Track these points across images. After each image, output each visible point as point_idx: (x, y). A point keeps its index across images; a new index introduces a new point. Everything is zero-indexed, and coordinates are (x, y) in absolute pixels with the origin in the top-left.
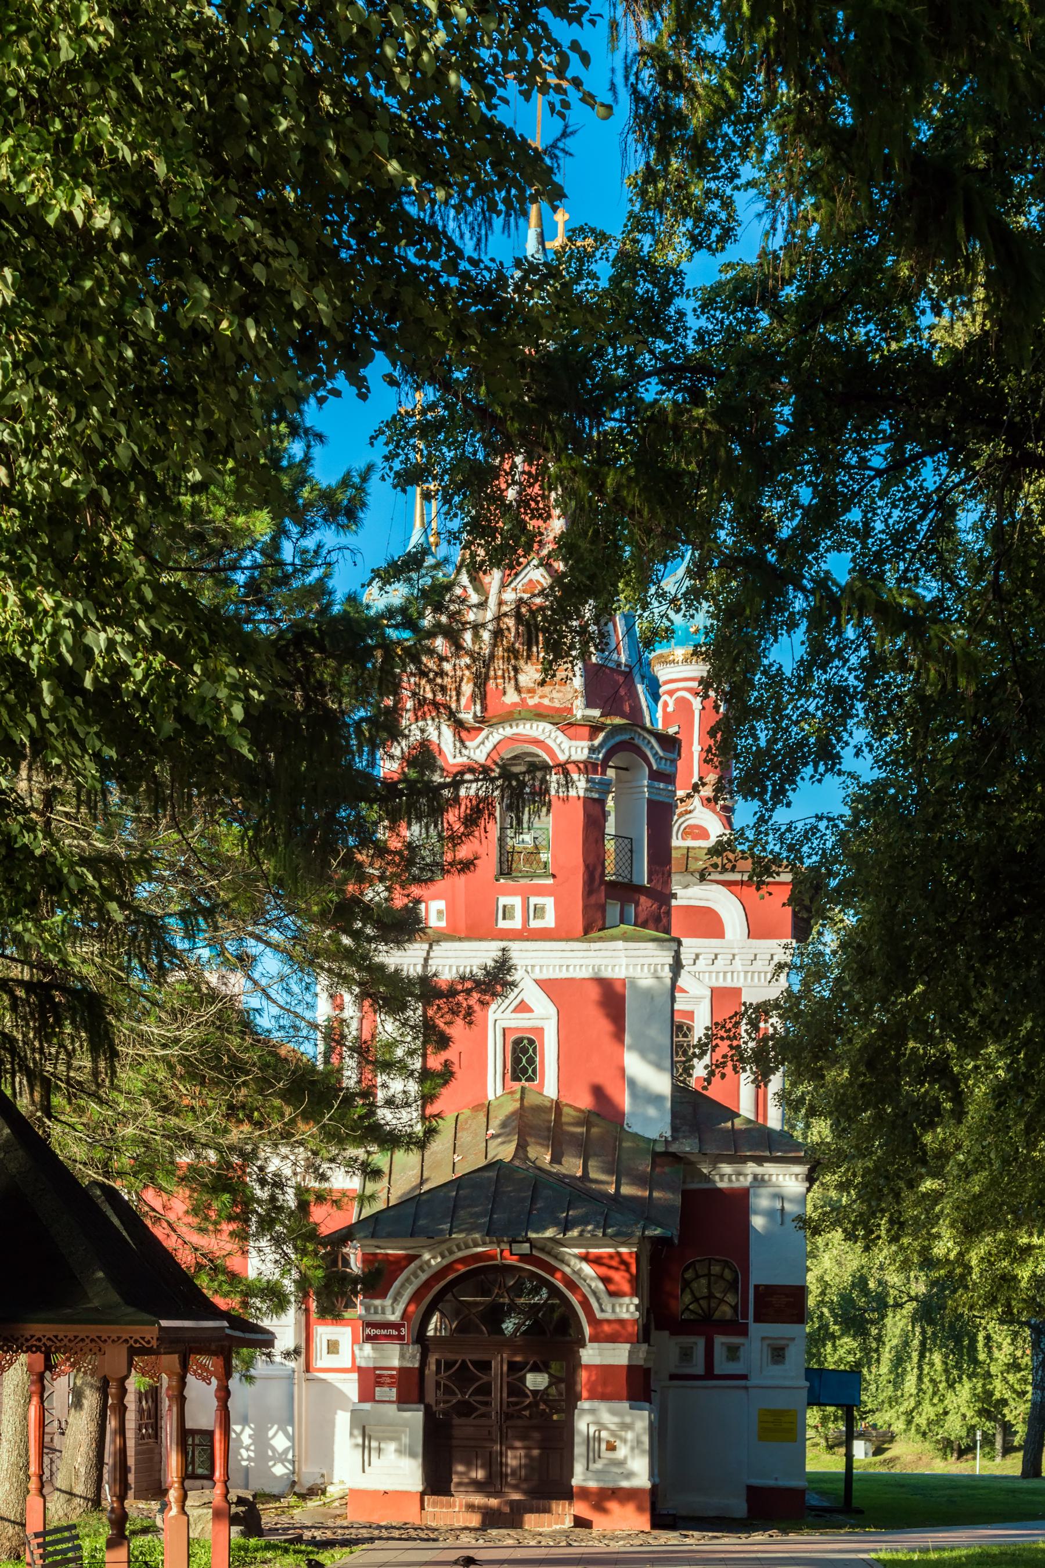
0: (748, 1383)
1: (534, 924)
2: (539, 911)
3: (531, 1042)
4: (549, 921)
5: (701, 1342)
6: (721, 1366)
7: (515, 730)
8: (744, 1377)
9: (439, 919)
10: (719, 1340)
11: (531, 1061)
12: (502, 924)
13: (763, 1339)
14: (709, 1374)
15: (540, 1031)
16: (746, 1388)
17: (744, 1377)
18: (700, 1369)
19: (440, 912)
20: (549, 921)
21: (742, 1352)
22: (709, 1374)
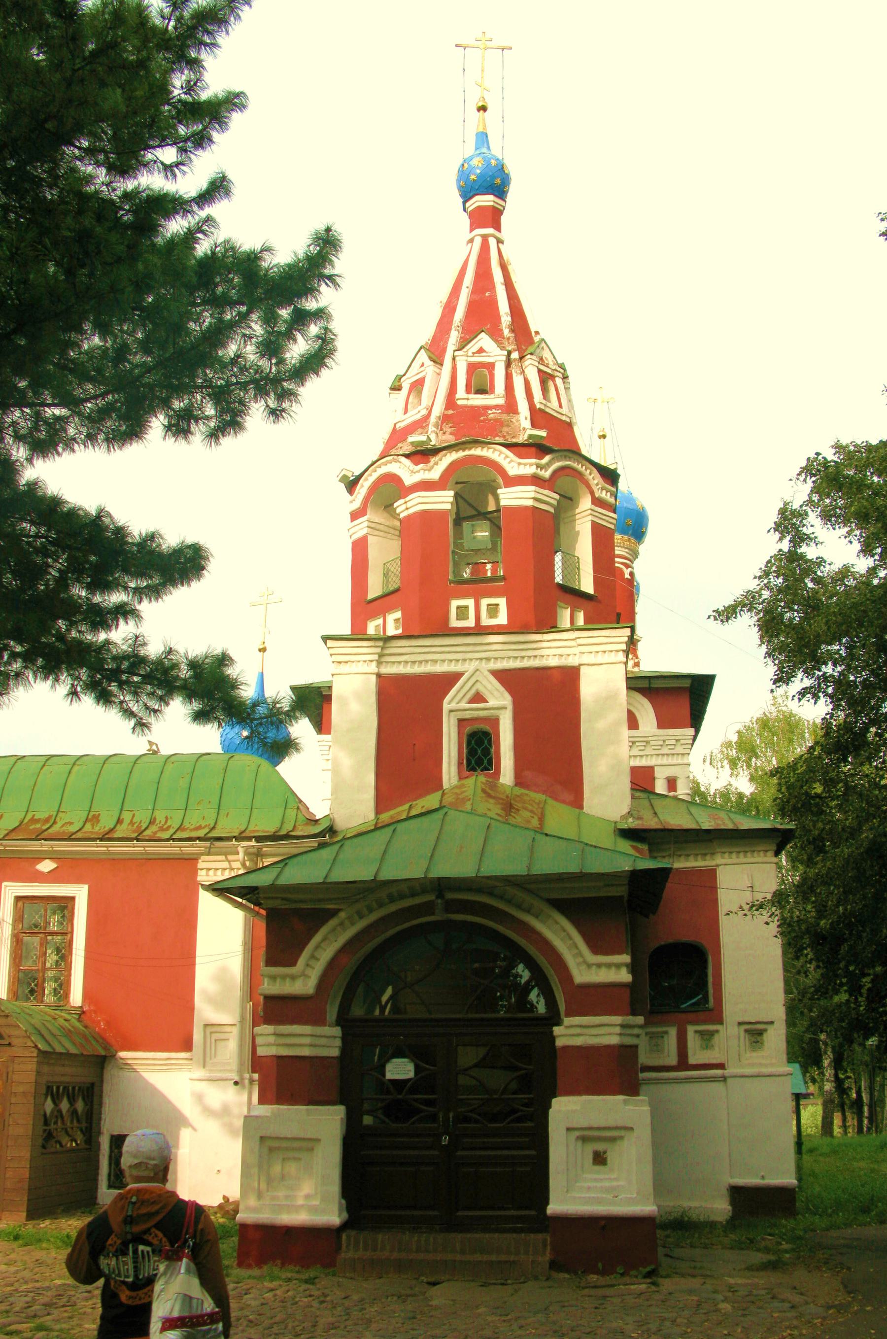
0: (726, 1072)
1: (486, 621)
2: (493, 610)
3: (486, 734)
4: (502, 619)
5: (673, 1032)
7: (467, 453)
8: (721, 1066)
9: (397, 628)
10: (691, 1030)
11: (487, 752)
12: (454, 623)
13: (740, 1024)
14: (683, 1064)
15: (495, 722)
16: (724, 1079)
17: (721, 1066)
18: (673, 1060)
19: (396, 620)
20: (502, 619)
22: (683, 1064)
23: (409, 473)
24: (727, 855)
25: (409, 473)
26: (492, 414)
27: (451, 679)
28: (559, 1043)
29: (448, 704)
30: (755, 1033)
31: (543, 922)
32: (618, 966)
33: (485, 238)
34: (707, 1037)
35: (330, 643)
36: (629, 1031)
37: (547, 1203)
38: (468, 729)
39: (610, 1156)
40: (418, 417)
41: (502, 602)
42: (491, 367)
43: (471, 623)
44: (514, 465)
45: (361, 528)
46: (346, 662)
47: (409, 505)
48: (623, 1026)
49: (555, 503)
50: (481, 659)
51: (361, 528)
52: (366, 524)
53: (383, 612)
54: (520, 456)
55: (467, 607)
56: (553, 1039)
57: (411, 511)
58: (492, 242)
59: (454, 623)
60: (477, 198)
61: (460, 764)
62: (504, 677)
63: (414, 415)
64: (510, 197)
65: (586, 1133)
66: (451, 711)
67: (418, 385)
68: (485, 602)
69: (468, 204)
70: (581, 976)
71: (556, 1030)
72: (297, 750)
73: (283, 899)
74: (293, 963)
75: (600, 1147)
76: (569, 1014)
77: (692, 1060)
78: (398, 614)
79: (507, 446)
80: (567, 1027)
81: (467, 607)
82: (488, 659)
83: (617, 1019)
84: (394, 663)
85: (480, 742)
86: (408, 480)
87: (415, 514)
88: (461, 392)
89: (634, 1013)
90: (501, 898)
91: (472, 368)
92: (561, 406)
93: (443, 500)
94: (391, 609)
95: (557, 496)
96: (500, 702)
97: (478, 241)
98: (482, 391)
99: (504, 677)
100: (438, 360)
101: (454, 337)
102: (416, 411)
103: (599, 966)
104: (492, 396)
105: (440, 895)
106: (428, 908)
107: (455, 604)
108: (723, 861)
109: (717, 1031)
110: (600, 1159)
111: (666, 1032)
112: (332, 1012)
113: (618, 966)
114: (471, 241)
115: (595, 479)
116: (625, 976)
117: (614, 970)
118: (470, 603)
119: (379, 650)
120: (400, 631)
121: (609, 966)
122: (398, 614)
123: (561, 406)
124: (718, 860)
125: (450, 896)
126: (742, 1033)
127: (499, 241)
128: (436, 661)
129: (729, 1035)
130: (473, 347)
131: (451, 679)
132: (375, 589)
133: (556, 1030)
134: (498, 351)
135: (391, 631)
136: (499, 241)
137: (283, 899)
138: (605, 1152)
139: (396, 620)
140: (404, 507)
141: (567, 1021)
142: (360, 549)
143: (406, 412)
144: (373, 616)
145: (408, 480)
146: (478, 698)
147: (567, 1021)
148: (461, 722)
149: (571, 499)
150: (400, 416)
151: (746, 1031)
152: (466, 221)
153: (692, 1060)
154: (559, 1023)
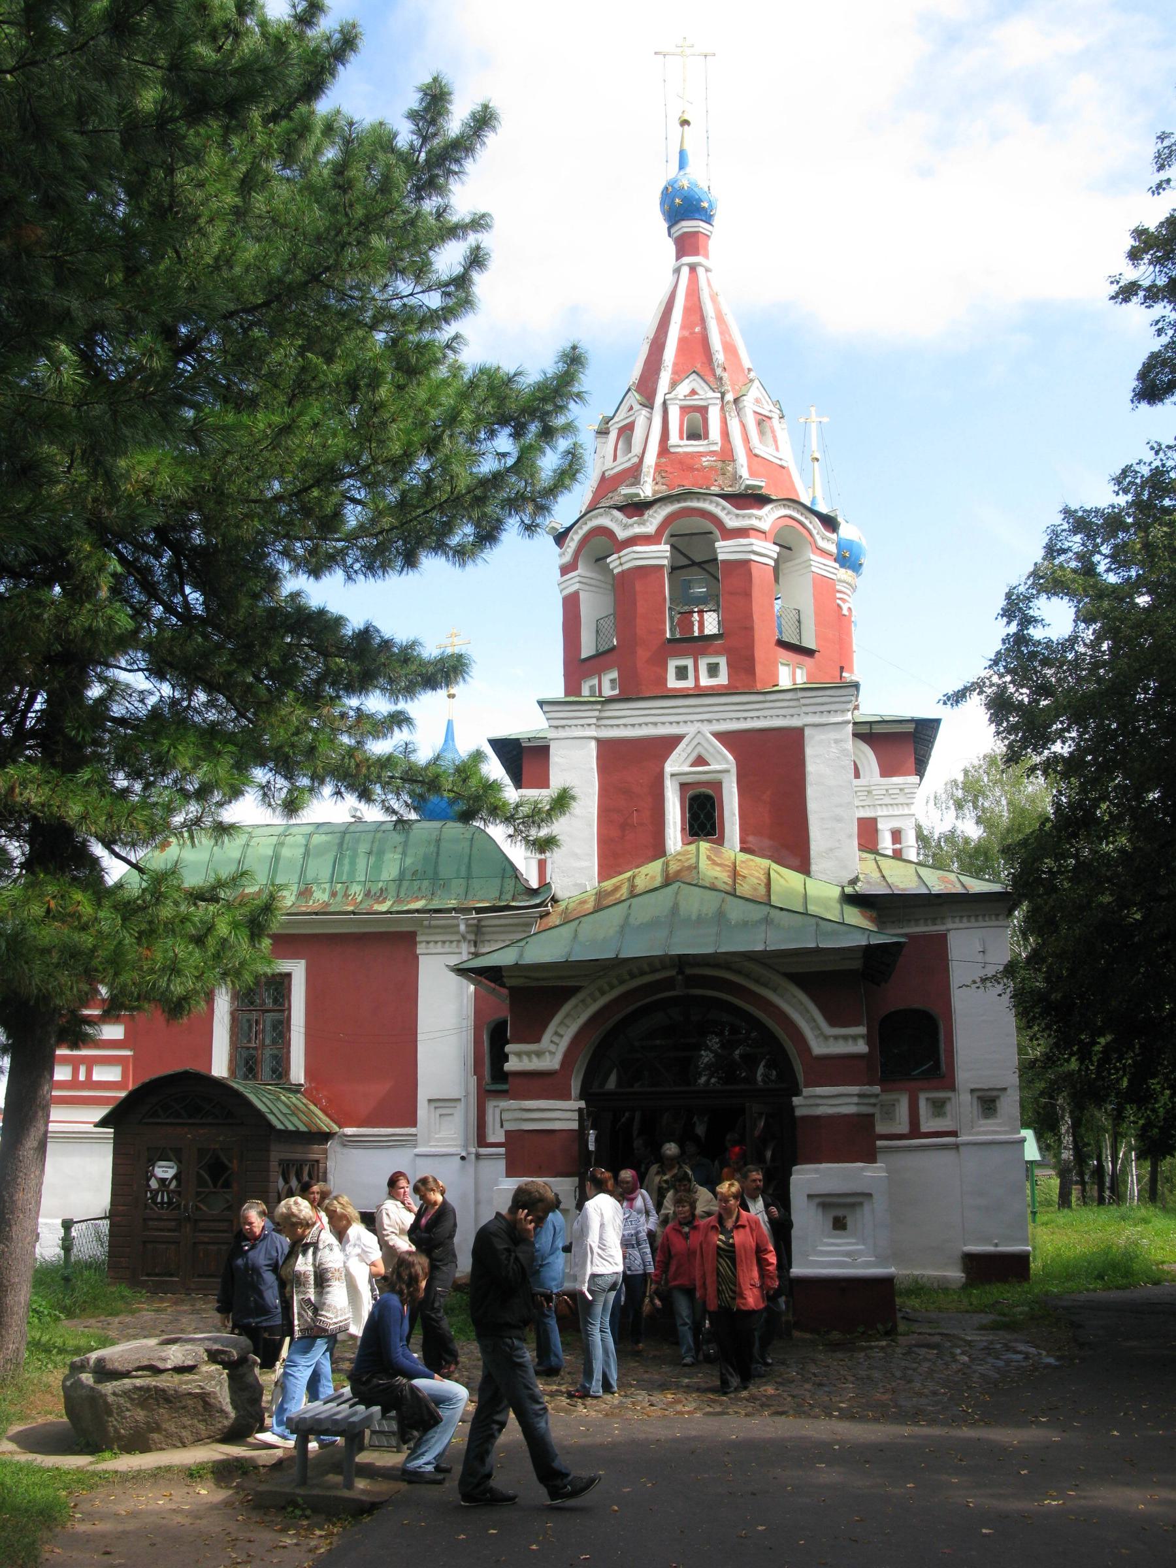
1: (705, 681)
4: (723, 679)
6: (928, 1124)
8: (954, 1134)
9: (613, 689)
12: (673, 683)
13: (972, 1091)
14: (915, 1131)
15: (718, 785)
16: (956, 1147)
17: (954, 1134)
18: (904, 1128)
19: (612, 681)
20: (723, 679)
21: (948, 1107)
22: (915, 1131)
23: (621, 526)
24: (957, 920)
25: (621, 526)
26: (706, 461)
27: (671, 742)
28: (799, 1112)
29: (670, 767)
30: (988, 1103)
31: (782, 996)
32: (855, 1038)
33: (693, 268)
34: (939, 1107)
35: (546, 708)
36: (866, 1101)
37: (790, 1267)
38: (691, 793)
39: (850, 1222)
40: (628, 465)
41: (722, 661)
42: (703, 410)
43: (689, 683)
44: (731, 518)
45: (573, 582)
46: (563, 727)
47: (623, 560)
48: (859, 1096)
49: (775, 556)
50: (702, 721)
51: (573, 582)
52: (578, 579)
53: (599, 672)
54: (738, 508)
55: (686, 668)
56: (792, 1109)
57: (626, 567)
58: (701, 271)
59: (673, 683)
60: (684, 223)
61: (683, 829)
62: (724, 737)
63: (624, 462)
64: (716, 221)
65: (828, 1200)
66: (672, 775)
67: (627, 430)
68: (703, 664)
69: (672, 231)
70: (819, 1048)
71: (796, 1100)
72: (558, 846)
73: (526, 977)
74: (537, 1040)
75: (840, 1213)
76: (806, 1086)
77: (924, 1128)
78: (614, 674)
79: (724, 497)
80: (805, 1098)
81: (686, 668)
82: (709, 721)
83: (855, 1089)
84: (612, 726)
85: (702, 806)
86: (621, 534)
87: (629, 569)
88: (674, 438)
89: (871, 1083)
90: (739, 972)
91: (684, 410)
92: (777, 449)
93: (660, 553)
94: (606, 668)
95: (777, 549)
96: (724, 763)
97: (685, 271)
98: (694, 435)
99: (724, 737)
100: (649, 404)
101: (665, 378)
102: (626, 458)
103: (836, 1038)
104: (706, 442)
105: (681, 972)
106: (669, 983)
107: (672, 664)
108: (955, 926)
109: (949, 1099)
110: (839, 1224)
111: (898, 1100)
112: (575, 1086)
113: (855, 1038)
114: (677, 271)
115: (815, 526)
116: (861, 1047)
117: (851, 1042)
118: (689, 662)
119: (596, 714)
120: (616, 692)
121: (845, 1038)
122: (614, 674)
123: (777, 449)
124: (950, 926)
125: (688, 971)
126: (975, 1101)
127: (707, 270)
128: (655, 724)
129: (963, 1102)
130: (684, 388)
131: (671, 742)
132: (587, 650)
133: (796, 1100)
134: (711, 394)
135: (608, 692)
136: (707, 270)
137: (526, 977)
138: (845, 1217)
139: (612, 681)
140: (617, 562)
141: (807, 1091)
142: (571, 605)
143: (615, 459)
144: (588, 675)
145: (621, 534)
146: (700, 761)
147: (807, 1091)
148: (683, 786)
149: (790, 549)
150: (609, 463)
151: (979, 1098)
152: (671, 248)
153: (924, 1128)
154: (798, 1093)
